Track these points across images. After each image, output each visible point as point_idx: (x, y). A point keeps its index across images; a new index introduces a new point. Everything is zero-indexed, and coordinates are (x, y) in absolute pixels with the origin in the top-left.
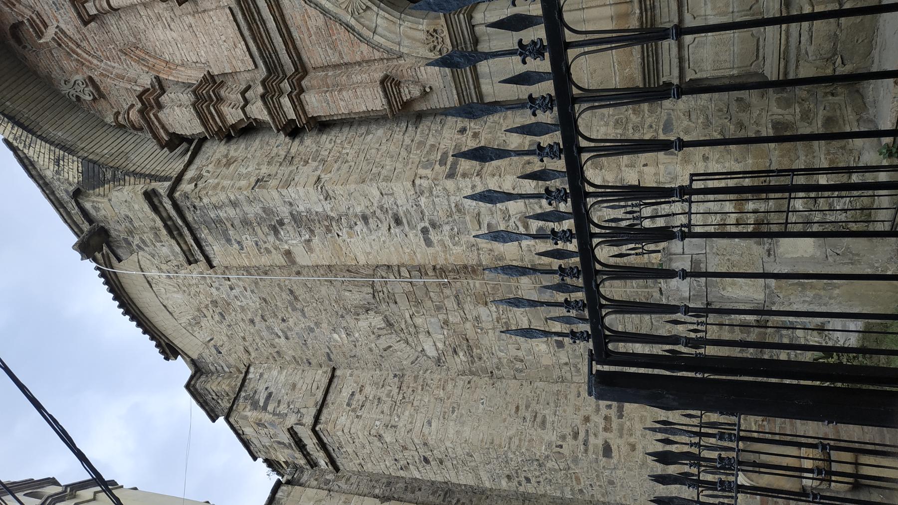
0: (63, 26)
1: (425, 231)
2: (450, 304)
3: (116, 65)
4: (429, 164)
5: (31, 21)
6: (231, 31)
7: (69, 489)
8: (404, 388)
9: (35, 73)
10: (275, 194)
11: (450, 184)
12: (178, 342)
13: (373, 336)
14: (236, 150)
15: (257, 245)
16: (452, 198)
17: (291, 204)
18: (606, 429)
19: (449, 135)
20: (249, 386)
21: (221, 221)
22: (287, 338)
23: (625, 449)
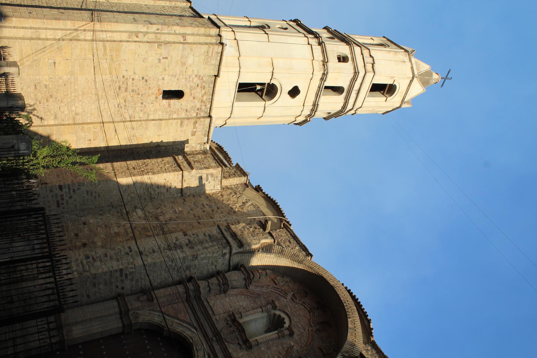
0: (285, 300)
1: (131, 251)
4: (131, 273)
5: (296, 299)
6: (215, 309)
7: (308, 119)
10: (188, 254)
11: (121, 267)
12: (254, 193)
13: (164, 212)
14: (213, 269)
15: (198, 236)
17: (182, 252)
18: (62, 195)
19: (128, 285)
20: (218, 182)
22: (203, 205)
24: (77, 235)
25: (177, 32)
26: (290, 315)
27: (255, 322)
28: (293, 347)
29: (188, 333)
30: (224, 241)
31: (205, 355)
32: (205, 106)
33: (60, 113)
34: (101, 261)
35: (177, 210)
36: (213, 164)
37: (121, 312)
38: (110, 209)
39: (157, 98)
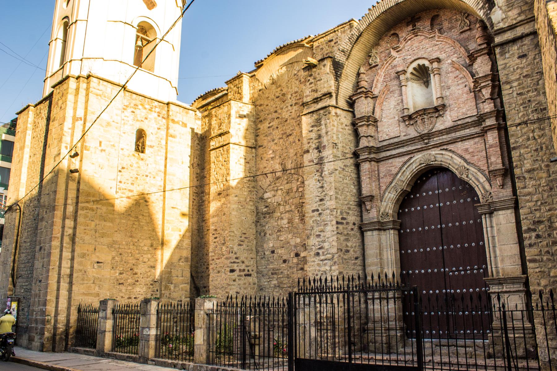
0: (397, 59)
1: (318, 210)
2: (288, 208)
3: (382, 79)
4: (341, 213)
5: (399, 47)
6: (392, 135)
8: (249, 183)
9: (380, 39)
10: (331, 152)
14: (349, 129)
16: (329, 223)
18: (240, 270)
19: (352, 218)
21: (320, 126)
22: (269, 127)
23: (234, 278)
24: (285, 261)
25: (70, 126)
26: (416, 57)
27: (415, 96)
28: (453, 62)
29: (414, 167)
30: (322, 112)
31: (442, 154)
32: (156, 107)
33: (149, 262)
34: (324, 241)
35: (271, 156)
36: (225, 108)
37: (379, 230)
38: (260, 225)
39: (142, 159)
